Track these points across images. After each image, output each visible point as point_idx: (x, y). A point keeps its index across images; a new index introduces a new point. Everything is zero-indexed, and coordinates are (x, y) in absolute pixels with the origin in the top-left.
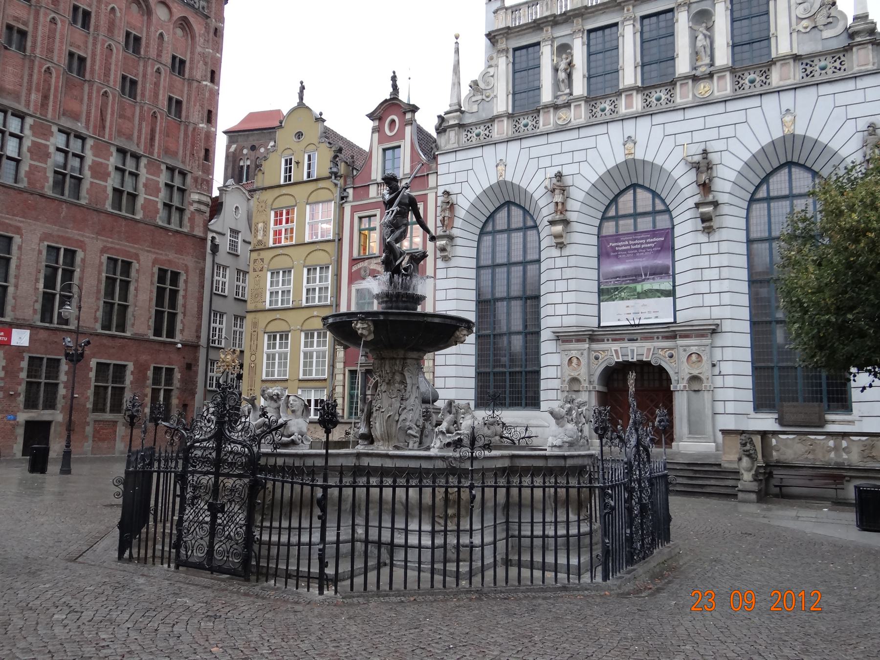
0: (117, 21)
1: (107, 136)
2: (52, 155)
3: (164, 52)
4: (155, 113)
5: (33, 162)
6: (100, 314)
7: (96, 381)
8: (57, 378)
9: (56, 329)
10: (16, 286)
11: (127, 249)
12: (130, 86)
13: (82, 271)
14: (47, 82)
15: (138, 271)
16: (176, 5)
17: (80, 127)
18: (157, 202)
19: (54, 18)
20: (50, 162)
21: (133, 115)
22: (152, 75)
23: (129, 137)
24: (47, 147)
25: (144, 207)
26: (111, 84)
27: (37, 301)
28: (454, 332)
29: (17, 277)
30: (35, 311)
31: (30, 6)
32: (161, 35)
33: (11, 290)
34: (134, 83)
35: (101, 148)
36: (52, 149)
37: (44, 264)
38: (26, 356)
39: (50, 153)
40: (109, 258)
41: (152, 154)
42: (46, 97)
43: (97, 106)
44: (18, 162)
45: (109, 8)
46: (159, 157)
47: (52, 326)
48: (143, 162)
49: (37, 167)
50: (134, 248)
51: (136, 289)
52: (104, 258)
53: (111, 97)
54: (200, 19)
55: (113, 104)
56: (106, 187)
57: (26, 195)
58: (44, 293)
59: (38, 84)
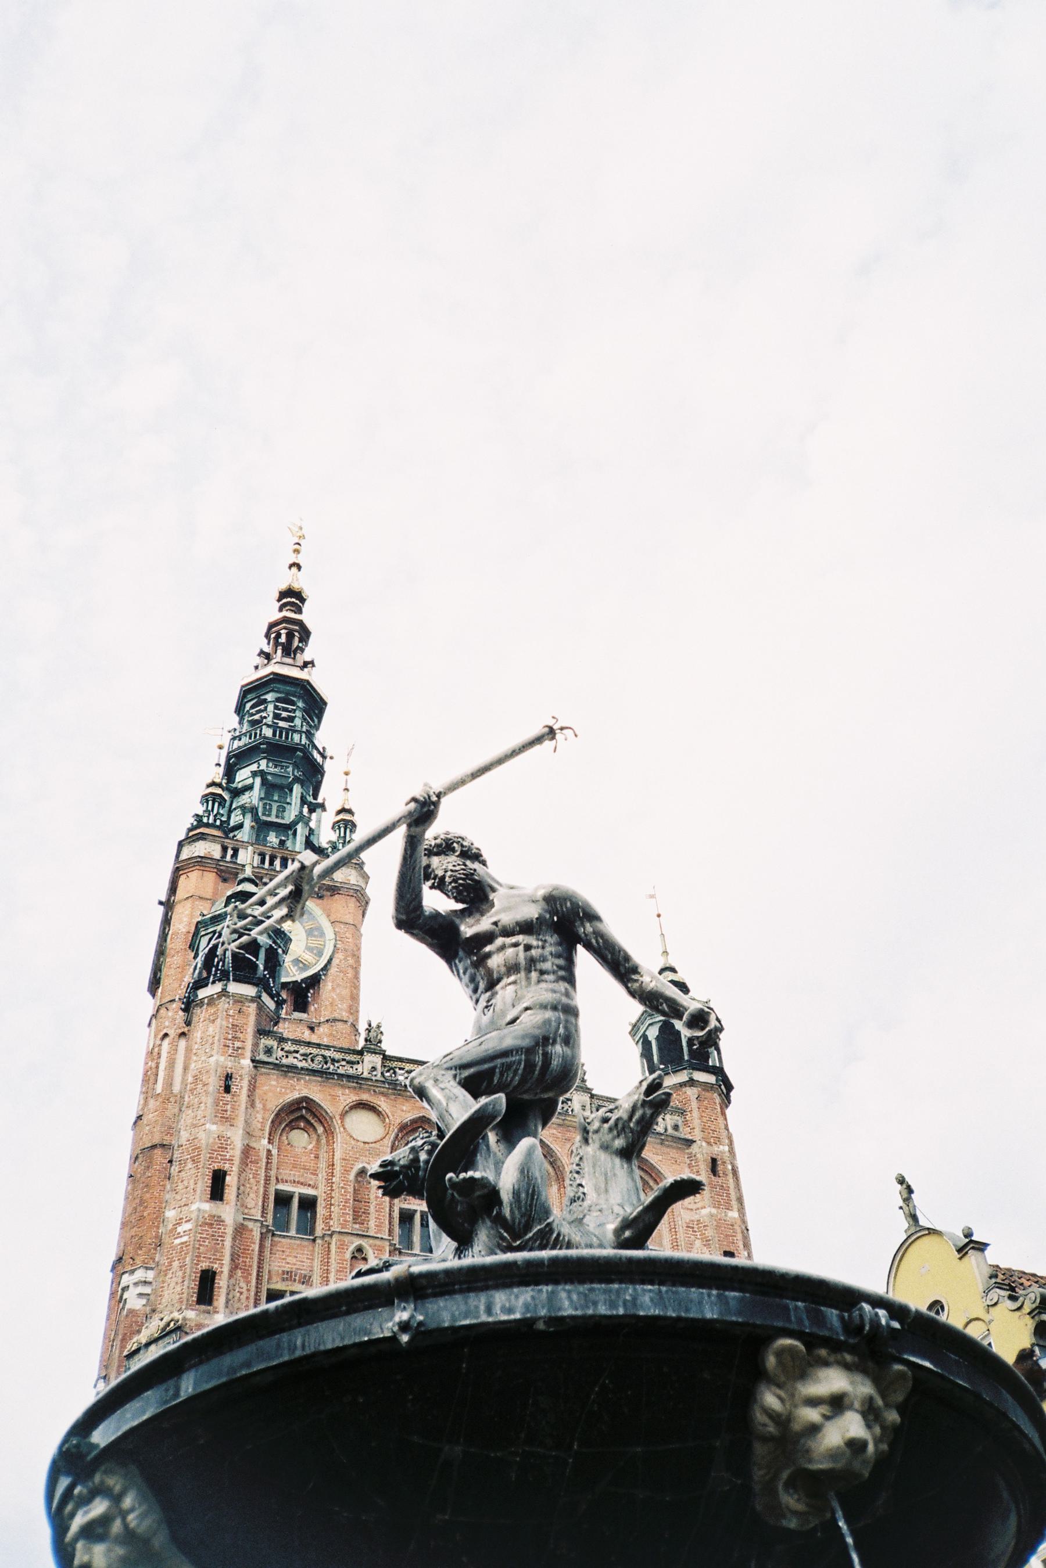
19: (360, 1250)
28: (747, 1397)
31: (314, 1240)
54: (673, 1153)
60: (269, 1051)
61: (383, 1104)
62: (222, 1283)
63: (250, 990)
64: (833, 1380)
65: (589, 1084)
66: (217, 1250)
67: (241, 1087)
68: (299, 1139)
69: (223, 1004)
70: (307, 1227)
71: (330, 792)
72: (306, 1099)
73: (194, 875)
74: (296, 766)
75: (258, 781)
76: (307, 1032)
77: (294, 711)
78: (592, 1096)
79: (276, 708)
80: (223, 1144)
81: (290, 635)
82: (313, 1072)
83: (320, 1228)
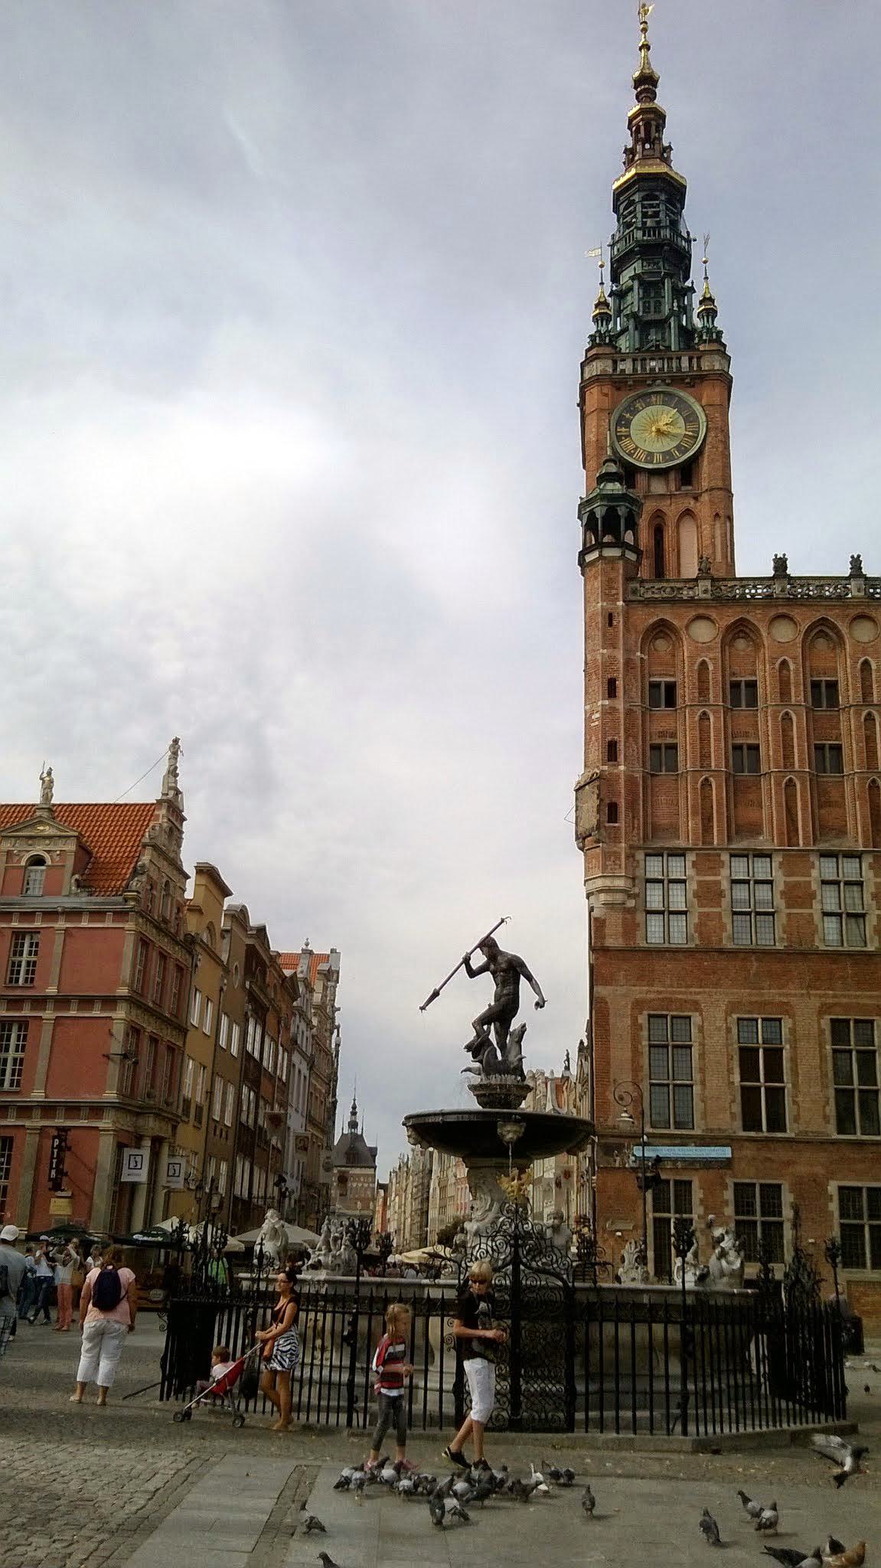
2: (727, 893)
6: (831, 1110)
7: (842, 1216)
8: (780, 1214)
9: (767, 1140)
10: (703, 1083)
11: (861, 1001)
13: (794, 1048)
14: (706, 797)
17: (763, 842)
19: (704, 713)
20: (725, 902)
22: (858, 728)
23: (842, 832)
24: (719, 882)
27: (733, 1101)
29: (702, 1070)
30: (733, 1115)
35: (795, 859)
36: (725, 885)
37: (736, 1046)
38: (730, 1182)
39: (722, 891)
42: (710, 819)
43: (779, 804)
44: (685, 913)
45: (777, 666)
47: (760, 1135)
49: (708, 914)
52: (825, 1023)
56: (811, 915)
58: (743, 1088)
59: (693, 806)
60: (635, 592)
62: (621, 746)
63: (615, 552)
65: (864, 571)
66: (616, 729)
67: (619, 621)
68: (661, 645)
69: (600, 565)
70: (671, 701)
71: (696, 277)
72: (662, 620)
76: (692, 502)
78: (866, 578)
79: (643, 207)
80: (612, 659)
81: (648, 127)
83: (679, 701)
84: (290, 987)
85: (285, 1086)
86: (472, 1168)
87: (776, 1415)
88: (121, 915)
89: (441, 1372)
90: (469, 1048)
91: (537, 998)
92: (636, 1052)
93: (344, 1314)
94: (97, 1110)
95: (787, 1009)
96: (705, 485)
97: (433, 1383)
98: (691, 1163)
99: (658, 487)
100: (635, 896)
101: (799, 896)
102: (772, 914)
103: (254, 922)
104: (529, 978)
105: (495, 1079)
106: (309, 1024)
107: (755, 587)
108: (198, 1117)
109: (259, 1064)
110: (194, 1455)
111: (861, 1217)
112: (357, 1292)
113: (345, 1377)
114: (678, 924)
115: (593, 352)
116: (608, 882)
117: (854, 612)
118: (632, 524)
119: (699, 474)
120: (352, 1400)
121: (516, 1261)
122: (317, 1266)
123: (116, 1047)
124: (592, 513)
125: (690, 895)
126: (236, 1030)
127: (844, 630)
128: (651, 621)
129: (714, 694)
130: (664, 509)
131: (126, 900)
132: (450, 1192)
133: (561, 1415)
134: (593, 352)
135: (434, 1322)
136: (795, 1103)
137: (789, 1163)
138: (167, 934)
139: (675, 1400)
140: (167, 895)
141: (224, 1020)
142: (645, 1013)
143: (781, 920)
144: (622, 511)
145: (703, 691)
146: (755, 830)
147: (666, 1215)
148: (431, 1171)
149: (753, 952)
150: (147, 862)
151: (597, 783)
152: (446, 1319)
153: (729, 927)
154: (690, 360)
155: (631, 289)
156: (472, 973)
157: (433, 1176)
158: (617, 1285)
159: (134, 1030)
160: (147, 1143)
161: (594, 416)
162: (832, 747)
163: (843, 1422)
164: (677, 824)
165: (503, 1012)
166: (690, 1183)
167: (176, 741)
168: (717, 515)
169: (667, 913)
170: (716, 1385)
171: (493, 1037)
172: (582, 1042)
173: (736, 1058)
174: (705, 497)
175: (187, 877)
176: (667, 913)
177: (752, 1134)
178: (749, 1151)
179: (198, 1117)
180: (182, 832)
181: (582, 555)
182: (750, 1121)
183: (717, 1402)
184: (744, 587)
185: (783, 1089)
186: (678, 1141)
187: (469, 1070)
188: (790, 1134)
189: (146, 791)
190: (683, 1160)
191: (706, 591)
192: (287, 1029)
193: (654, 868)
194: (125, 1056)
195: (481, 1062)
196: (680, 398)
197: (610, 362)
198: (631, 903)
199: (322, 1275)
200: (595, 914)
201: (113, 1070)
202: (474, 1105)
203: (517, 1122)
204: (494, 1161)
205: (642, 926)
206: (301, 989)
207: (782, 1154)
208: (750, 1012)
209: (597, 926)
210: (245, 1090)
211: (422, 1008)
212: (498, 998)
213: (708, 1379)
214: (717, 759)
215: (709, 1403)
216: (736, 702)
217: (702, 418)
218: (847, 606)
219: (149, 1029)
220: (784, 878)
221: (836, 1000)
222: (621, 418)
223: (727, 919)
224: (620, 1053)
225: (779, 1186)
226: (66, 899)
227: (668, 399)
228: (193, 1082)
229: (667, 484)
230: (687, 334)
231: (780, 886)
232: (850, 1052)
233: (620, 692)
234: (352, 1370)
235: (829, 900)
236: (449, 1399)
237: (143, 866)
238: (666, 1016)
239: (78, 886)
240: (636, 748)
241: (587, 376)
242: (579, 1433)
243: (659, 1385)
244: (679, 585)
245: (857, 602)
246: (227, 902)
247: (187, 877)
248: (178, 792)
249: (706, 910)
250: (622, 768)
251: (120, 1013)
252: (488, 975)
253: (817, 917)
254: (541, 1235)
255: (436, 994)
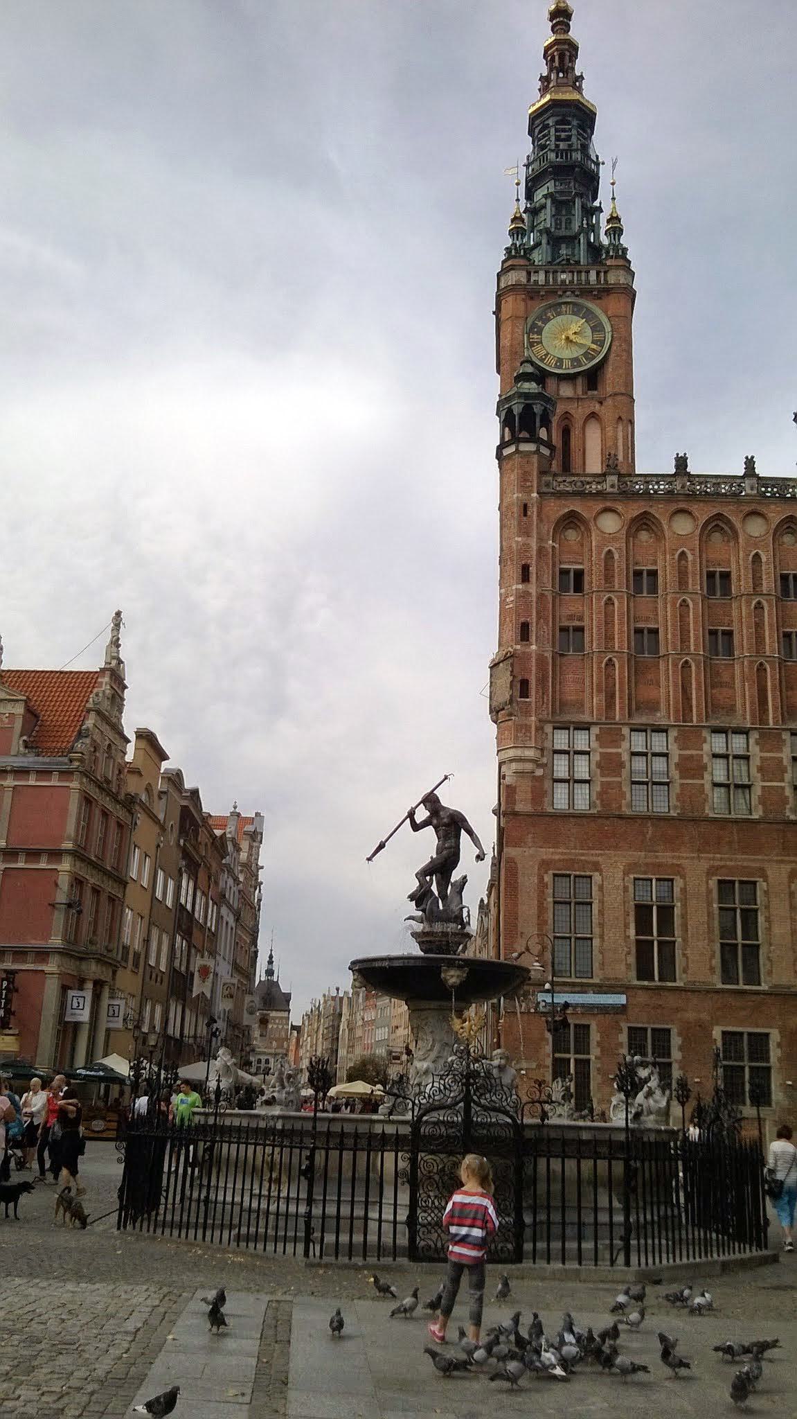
0: (690, 567)
1: (695, 719)
2: (627, 765)
3: (764, 577)
4: (761, 664)
5: (604, 779)
6: (717, 962)
8: (669, 1055)
10: (602, 937)
11: (745, 864)
12: (720, 640)
13: (684, 906)
14: (609, 677)
15: (766, 893)
16: (773, 507)
17: (660, 718)
18: (783, 788)
19: (610, 599)
21: (733, 678)
22: (749, 615)
23: (731, 709)
25: (762, 801)
26: (692, 648)
29: (601, 925)
30: (628, 966)
32: (757, 555)
33: (596, 942)
34: (729, 634)
35: (690, 736)
36: (625, 757)
38: (624, 1026)
40: (720, 882)
41: (763, 721)
42: (613, 696)
43: (676, 685)
44: (588, 782)
45: (676, 556)
46: (776, 723)
47: (652, 984)
48: (754, 736)
49: (609, 783)
50: (754, 860)
51: (768, 920)
52: (713, 883)
53: (693, 668)
55: (698, 674)
57: (600, 821)
58: (638, 941)
60: (547, 485)
61: (620, 508)
62: (533, 628)
63: (530, 447)
64: (452, 972)
67: (533, 511)
68: (571, 535)
70: (579, 588)
71: (603, 199)
73: (510, 299)
74: (575, 180)
75: (549, 202)
76: (597, 406)
77: (570, 130)
78: (759, 478)
79: (557, 130)
80: (525, 548)
81: (562, 56)
82: (575, 494)
83: (586, 587)
84: (219, 845)
85: (214, 936)
86: (413, 1010)
87: (706, 1246)
88: (66, 774)
89: (395, 1205)
90: (412, 897)
91: (477, 852)
92: (541, 909)
93: (301, 1148)
94: (43, 955)
95: (679, 870)
96: (609, 390)
97: (388, 1215)
98: (590, 1009)
99: (566, 390)
100: (543, 766)
101: (692, 768)
102: (667, 784)
103: (188, 785)
104: (470, 832)
105: (438, 927)
106: (236, 880)
107: (657, 483)
108: (136, 965)
109: (191, 915)
110: (165, 1290)
111: (741, 1059)
112: (314, 1128)
113: (303, 1209)
114: (582, 793)
115: (510, 263)
116: (518, 752)
117: (747, 509)
118: (546, 422)
119: (603, 378)
120: (309, 1230)
121: (467, 1099)
122: (270, 1102)
123: (61, 897)
124: (510, 410)
125: (593, 766)
126: (171, 884)
127: (738, 525)
128: (562, 513)
129: (619, 582)
130: (572, 412)
131: (71, 761)
132: (359, 1033)
133: (510, 1246)
134: (510, 263)
135: (389, 1157)
136: (684, 955)
137: (677, 1010)
138: (109, 793)
139: (620, 1231)
140: (110, 757)
141: (161, 874)
142: (551, 872)
143: (675, 789)
144: (537, 409)
145: (608, 577)
146: (653, 707)
147: (567, 1056)
148: (340, 1015)
149: (649, 818)
150: (91, 726)
151: (511, 661)
152: (400, 1154)
153: (628, 796)
154: (598, 273)
155: (543, 207)
156: (416, 827)
157: (343, 1019)
158: (603, 1124)
159: (78, 882)
160: (90, 985)
161: (509, 323)
162: (725, 633)
163: (765, 1252)
164: (583, 700)
165: (444, 865)
166: (588, 1026)
167: (118, 614)
168: (620, 418)
169: (571, 781)
170: (649, 1217)
171: (434, 888)
172: (482, 901)
173: (632, 913)
174: (609, 402)
175: (128, 741)
176: (571, 781)
177: (646, 983)
178: (642, 997)
179: (136, 965)
180: (123, 699)
181: (500, 449)
182: (644, 971)
183: (649, 1234)
184: (647, 482)
185: (674, 942)
186: (577, 989)
187: (411, 918)
188: (679, 984)
189: (92, 662)
190: (583, 1005)
191: (612, 486)
192: (216, 883)
193: (561, 740)
194: (69, 906)
195: (424, 911)
196: (588, 309)
197: (524, 273)
198: (539, 772)
199: (276, 1111)
200: (508, 780)
201: (58, 919)
202: (417, 951)
203: (460, 967)
204: (434, 1004)
205: (550, 792)
206: (230, 848)
207: (671, 1001)
208: (645, 873)
209: (507, 792)
210: (178, 938)
211: (369, 859)
212: (439, 850)
213: (641, 1211)
214: (621, 640)
215: (642, 1235)
216: (638, 590)
217: (608, 328)
218: (739, 502)
219: (92, 881)
220: (678, 752)
221: (722, 863)
222: (534, 325)
223: (626, 789)
224: (527, 908)
225: (669, 1031)
226: (15, 759)
227: (577, 310)
228: (131, 930)
229: (575, 389)
230: (595, 250)
231: (675, 759)
232: (734, 910)
233: (533, 578)
234: (310, 1201)
235: (719, 772)
236: (403, 1230)
237: (87, 729)
238: (569, 876)
239: (26, 747)
240: (547, 630)
241: (502, 285)
242: (527, 1264)
243: (603, 1218)
244: (588, 479)
245: (750, 499)
246: (165, 765)
247: (128, 741)
248: (120, 662)
249: (609, 779)
250: (534, 647)
251: (66, 865)
252: (430, 829)
253: (708, 786)
254: (488, 1074)
255: (382, 846)
